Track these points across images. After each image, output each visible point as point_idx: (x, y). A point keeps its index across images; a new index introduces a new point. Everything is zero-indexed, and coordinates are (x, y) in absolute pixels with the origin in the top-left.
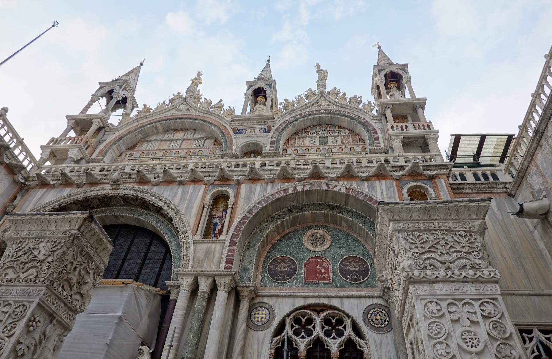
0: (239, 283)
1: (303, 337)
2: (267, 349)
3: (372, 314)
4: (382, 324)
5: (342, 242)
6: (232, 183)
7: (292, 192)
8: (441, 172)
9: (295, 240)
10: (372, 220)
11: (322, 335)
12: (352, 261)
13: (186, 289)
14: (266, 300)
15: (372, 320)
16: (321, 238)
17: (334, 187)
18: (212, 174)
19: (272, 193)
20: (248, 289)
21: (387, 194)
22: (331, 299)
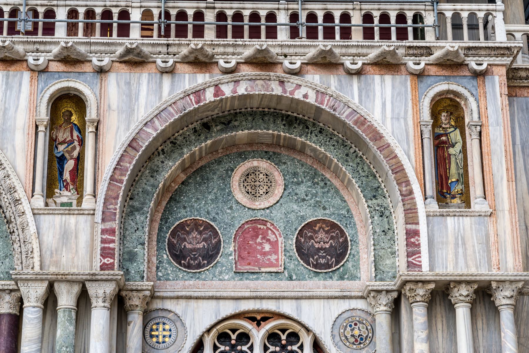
3: (346, 326)
4: (360, 343)
5: (302, 190)
6: (87, 68)
7: (212, 99)
8: (498, 60)
9: (215, 183)
10: (361, 153)
12: (320, 228)
13: (35, 304)
14: (169, 305)
15: (346, 337)
18: (42, 48)
20: (141, 295)
21: (393, 111)
22: (281, 301)
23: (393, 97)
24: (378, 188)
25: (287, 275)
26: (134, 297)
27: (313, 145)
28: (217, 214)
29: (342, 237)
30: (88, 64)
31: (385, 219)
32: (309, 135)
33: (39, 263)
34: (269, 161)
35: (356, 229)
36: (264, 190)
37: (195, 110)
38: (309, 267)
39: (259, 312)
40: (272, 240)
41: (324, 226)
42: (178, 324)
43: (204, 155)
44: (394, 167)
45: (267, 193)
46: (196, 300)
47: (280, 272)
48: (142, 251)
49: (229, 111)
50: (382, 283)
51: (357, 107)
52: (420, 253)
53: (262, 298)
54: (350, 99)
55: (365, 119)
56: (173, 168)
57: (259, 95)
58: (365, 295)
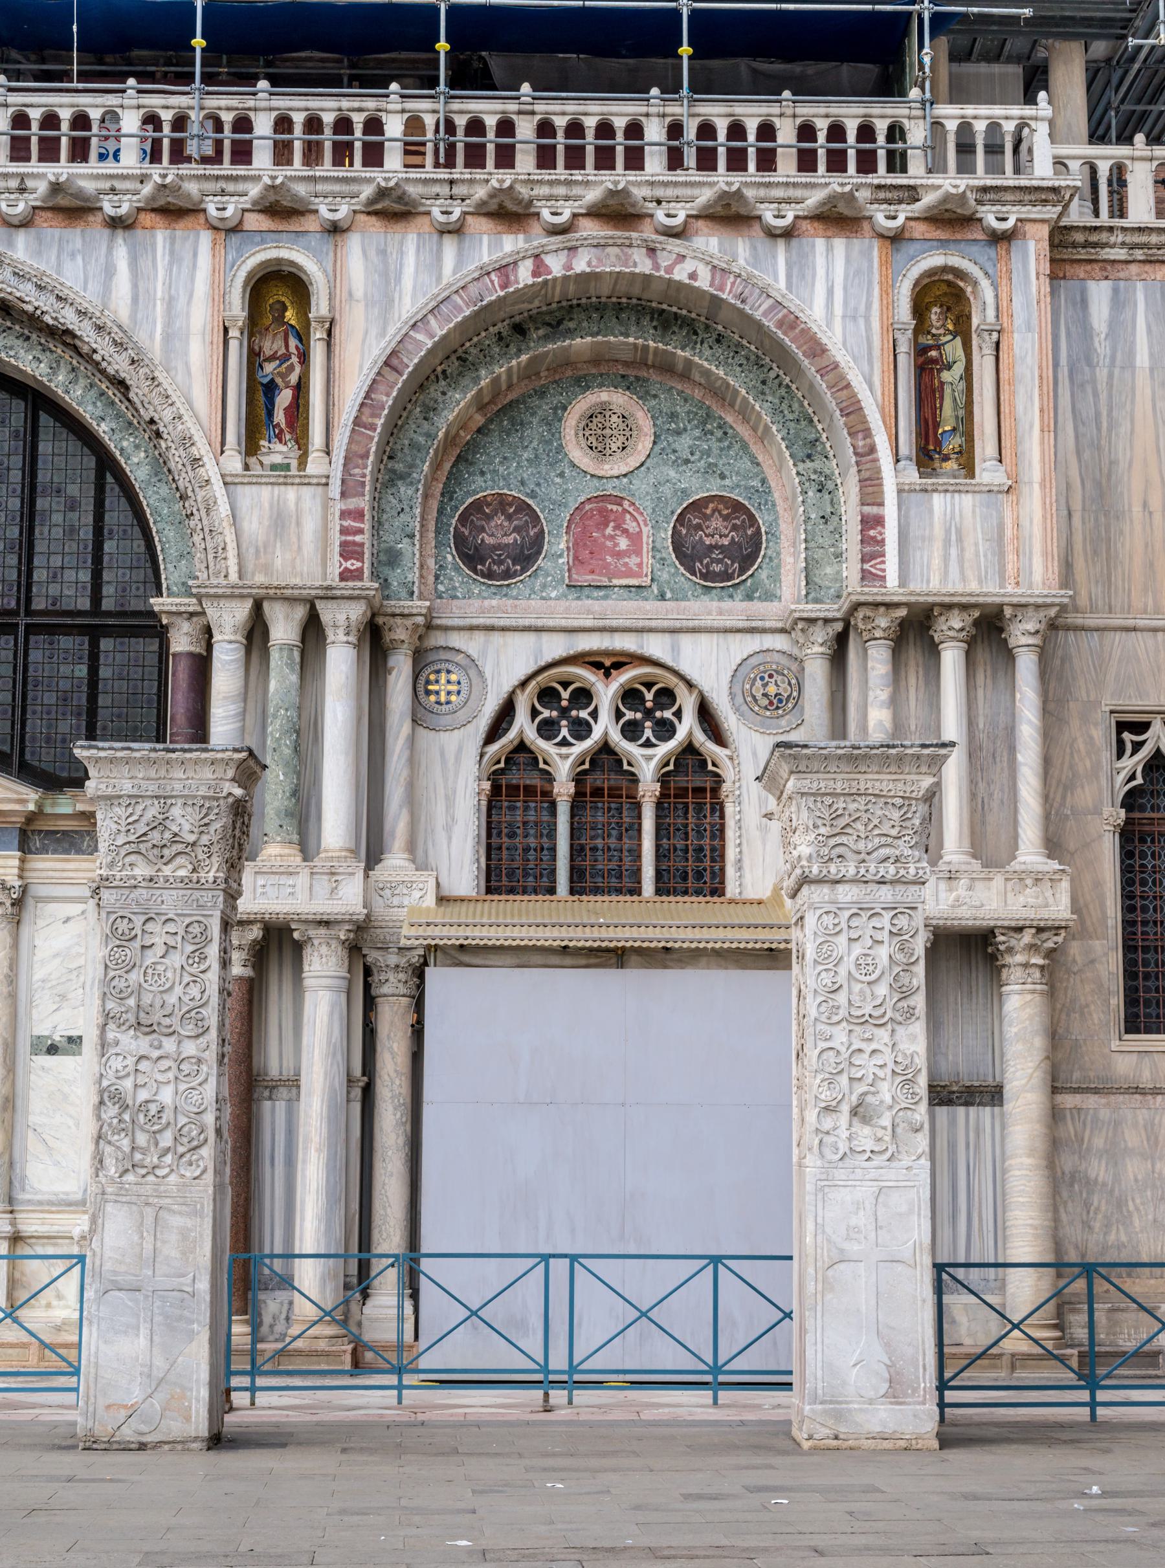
1: (564, 743)
2: (471, 779)
3: (755, 679)
5: (684, 443)
6: (310, 224)
7: (530, 281)
8: (1036, 212)
9: (535, 430)
10: (787, 380)
11: (616, 737)
12: (714, 511)
13: (232, 638)
14: (456, 640)
15: (754, 697)
17: (676, 263)
18: (230, 187)
20: (409, 622)
21: (846, 303)
27: (706, 364)
28: (538, 484)
29: (751, 526)
30: (312, 217)
31: (827, 497)
33: (236, 568)
36: (619, 444)
37: (500, 300)
39: (607, 653)
41: (721, 507)
42: (473, 673)
43: (515, 380)
50: (818, 606)
53: (613, 630)
54: (770, 281)
56: (462, 404)
58: (788, 627)
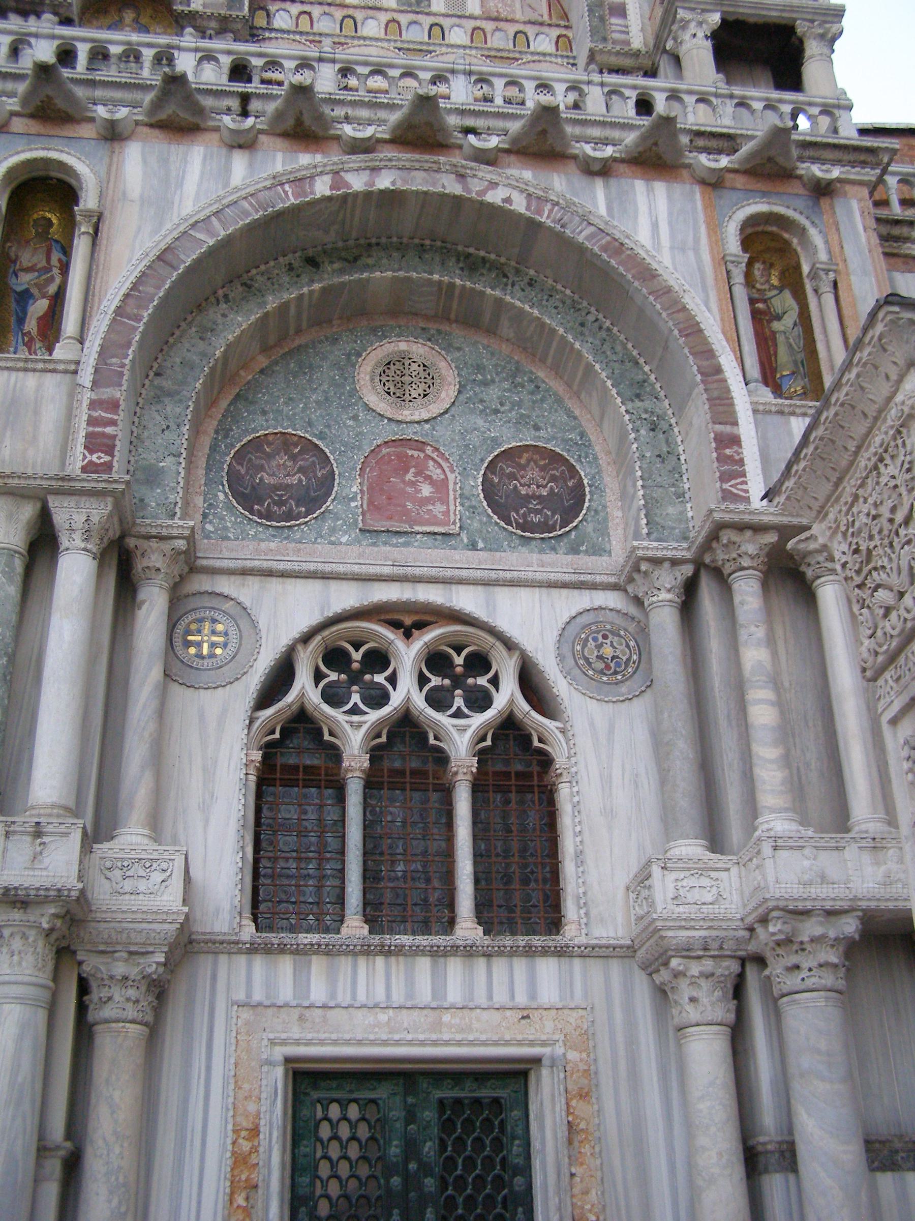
0: (134, 524)
1: (355, 711)
2: (238, 746)
3: (586, 640)
4: (616, 673)
5: (493, 393)
6: (87, 131)
7: (328, 193)
8: (854, 173)
10: (608, 323)
11: (419, 701)
12: (529, 461)
14: (225, 585)
15: (587, 660)
16: (422, 375)
19: (251, 190)
20: (167, 546)
21: (672, 236)
22: (454, 587)
23: (670, 214)
24: (644, 381)
25: (465, 540)
26: (153, 552)
28: (329, 426)
29: (571, 478)
32: (509, 287)
34: (429, 343)
35: (598, 466)
36: (421, 391)
38: (510, 528)
40: (435, 477)
41: (536, 457)
42: (244, 624)
43: (304, 325)
44: (682, 326)
45: (425, 396)
46: (280, 579)
47: (453, 534)
48: (174, 468)
49: (357, 239)
51: (607, 223)
52: (744, 476)
54: (591, 209)
55: (622, 244)
57: (417, 193)
